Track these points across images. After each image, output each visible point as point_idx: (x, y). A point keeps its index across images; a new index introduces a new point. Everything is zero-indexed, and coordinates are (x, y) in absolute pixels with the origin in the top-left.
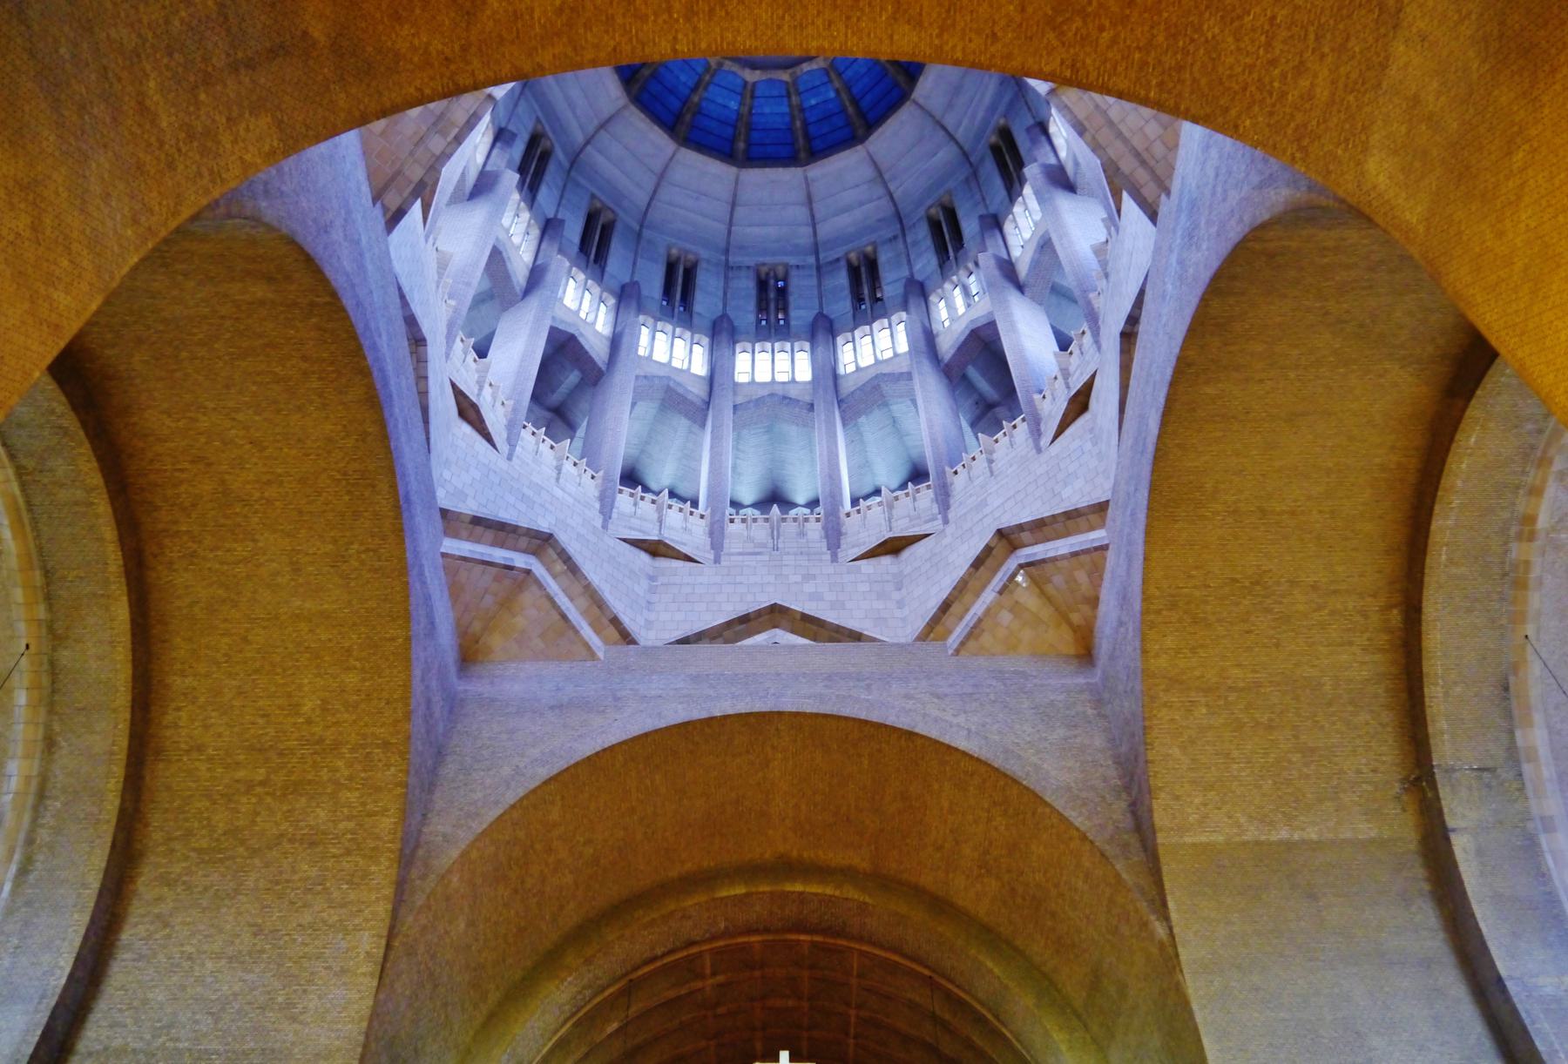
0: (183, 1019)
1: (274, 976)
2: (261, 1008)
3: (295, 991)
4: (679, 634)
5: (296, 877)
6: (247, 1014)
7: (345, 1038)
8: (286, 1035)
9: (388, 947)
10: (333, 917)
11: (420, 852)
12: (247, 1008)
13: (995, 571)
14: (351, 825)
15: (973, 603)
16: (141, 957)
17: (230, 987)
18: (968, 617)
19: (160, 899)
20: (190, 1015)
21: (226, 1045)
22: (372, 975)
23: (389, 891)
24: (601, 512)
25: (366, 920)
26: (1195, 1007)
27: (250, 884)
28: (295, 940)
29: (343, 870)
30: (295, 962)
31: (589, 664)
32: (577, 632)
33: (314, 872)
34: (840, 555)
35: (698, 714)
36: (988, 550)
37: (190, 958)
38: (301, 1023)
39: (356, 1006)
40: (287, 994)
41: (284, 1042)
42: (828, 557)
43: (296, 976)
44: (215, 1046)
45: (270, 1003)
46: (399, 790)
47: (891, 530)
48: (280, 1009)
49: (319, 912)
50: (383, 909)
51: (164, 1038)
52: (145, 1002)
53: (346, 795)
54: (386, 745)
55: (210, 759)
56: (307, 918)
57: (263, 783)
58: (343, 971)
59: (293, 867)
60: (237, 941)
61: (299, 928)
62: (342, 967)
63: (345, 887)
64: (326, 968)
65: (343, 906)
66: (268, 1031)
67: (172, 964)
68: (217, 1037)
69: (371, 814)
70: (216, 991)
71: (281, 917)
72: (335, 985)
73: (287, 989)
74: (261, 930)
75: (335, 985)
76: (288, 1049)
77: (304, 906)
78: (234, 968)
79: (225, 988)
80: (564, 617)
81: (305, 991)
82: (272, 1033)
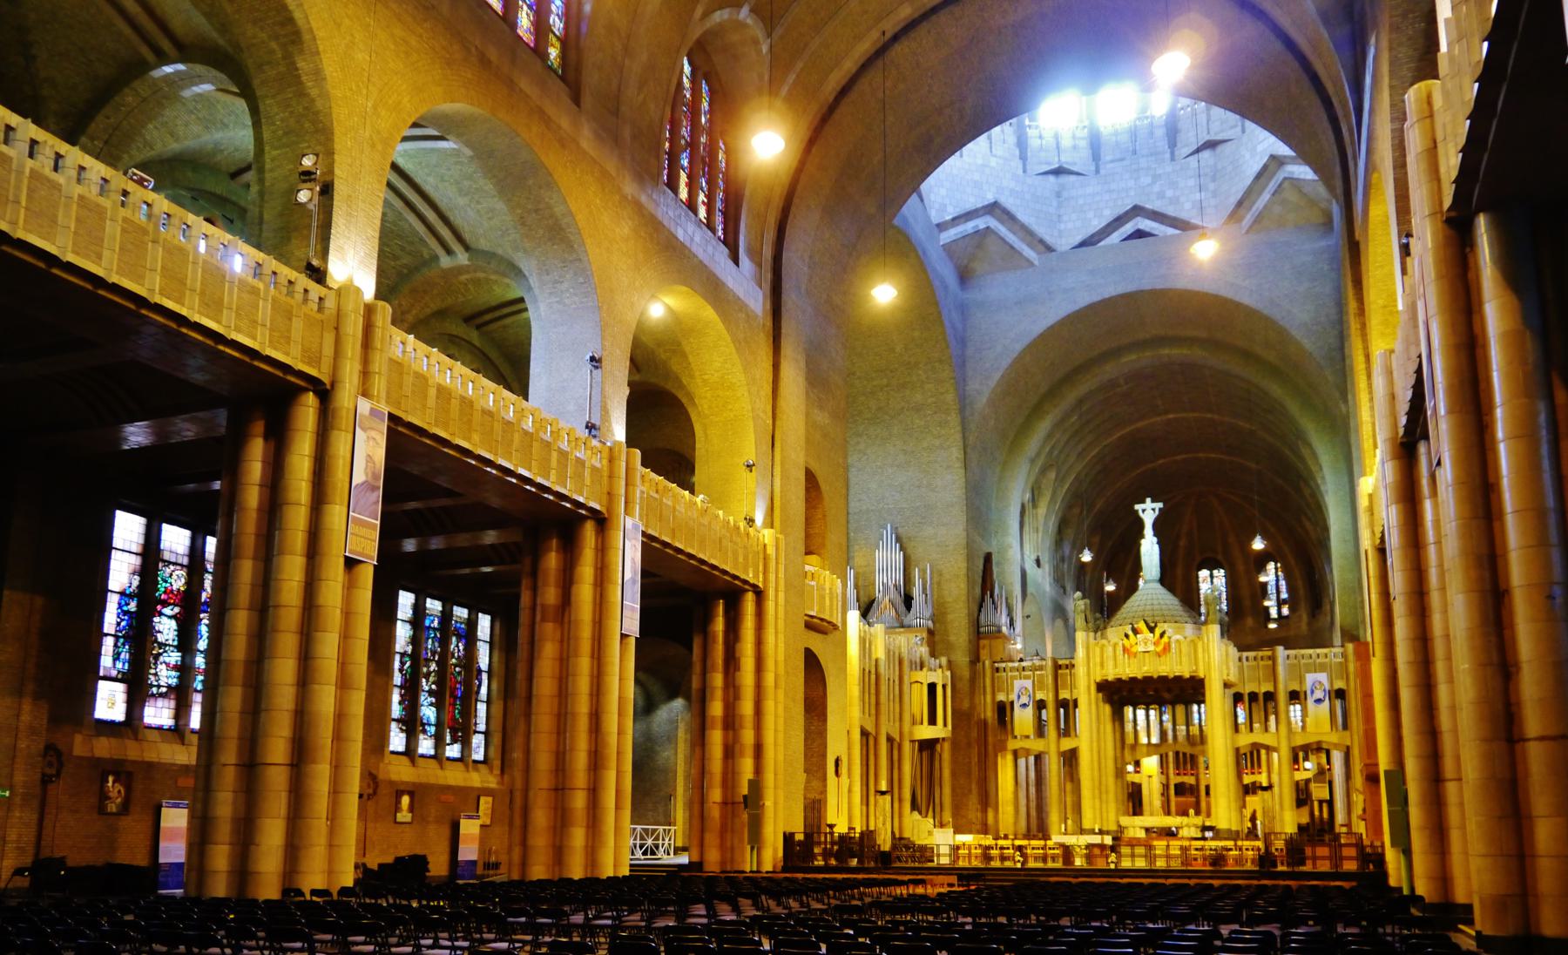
4: (1078, 239)
9: (965, 453)
10: (937, 442)
11: (967, 401)
13: (1270, 179)
14: (933, 399)
15: (1257, 200)
16: (859, 470)
18: (1254, 209)
19: (858, 443)
23: (959, 428)
24: (1021, 158)
27: (895, 431)
31: (1030, 270)
32: (1020, 254)
33: (923, 423)
34: (1177, 153)
35: (1096, 298)
36: (1265, 167)
37: (880, 468)
42: (1168, 156)
44: (904, 506)
46: (952, 381)
47: (1209, 133)
50: (958, 436)
52: (869, 489)
53: (928, 386)
54: (941, 361)
55: (859, 378)
56: (925, 444)
57: (887, 386)
58: (948, 467)
69: (942, 394)
80: (1012, 247)
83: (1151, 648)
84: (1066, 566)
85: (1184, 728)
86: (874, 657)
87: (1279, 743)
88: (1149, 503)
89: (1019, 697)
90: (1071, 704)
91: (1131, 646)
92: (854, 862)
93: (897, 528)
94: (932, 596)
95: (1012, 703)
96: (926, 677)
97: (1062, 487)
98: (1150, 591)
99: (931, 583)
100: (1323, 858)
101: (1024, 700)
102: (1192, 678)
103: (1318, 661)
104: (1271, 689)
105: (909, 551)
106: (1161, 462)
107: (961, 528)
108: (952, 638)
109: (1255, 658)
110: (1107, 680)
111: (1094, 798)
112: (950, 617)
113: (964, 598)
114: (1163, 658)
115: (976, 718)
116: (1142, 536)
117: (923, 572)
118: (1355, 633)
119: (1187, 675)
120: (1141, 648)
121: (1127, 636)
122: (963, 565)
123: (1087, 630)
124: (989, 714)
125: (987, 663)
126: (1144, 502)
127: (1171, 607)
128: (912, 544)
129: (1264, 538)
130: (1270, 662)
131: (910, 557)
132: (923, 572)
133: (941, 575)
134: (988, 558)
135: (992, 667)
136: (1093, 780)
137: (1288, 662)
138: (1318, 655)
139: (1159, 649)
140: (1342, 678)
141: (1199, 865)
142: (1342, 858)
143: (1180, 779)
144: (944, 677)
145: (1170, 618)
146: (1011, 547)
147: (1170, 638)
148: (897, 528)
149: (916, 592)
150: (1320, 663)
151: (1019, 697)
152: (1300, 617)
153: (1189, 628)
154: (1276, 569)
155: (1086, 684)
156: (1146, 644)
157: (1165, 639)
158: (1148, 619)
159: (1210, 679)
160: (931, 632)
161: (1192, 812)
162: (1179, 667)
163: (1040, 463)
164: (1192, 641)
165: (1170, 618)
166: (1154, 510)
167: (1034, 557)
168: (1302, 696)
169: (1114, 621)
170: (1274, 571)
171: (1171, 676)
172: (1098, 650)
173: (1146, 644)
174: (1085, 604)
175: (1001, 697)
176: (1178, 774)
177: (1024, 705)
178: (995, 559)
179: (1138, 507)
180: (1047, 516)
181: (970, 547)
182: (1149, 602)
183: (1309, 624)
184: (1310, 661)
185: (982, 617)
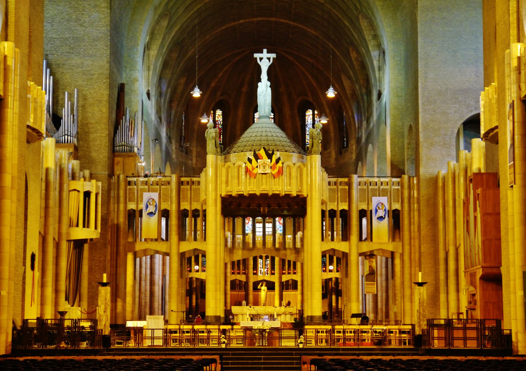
1: (69, 8)
3: (79, 14)
6: (63, 23)
8: (80, 32)
12: (62, 20)
17: (53, 12)
22: (107, 7)
26: (419, 25)
30: (75, 2)
38: (84, 27)
39: (103, 20)
41: (80, 34)
43: (78, 8)
44: (54, 36)
45: (70, 18)
58: (96, 6)
62: (95, 4)
64: (88, 5)
66: (73, 30)
68: (55, 32)
70: (48, 13)
72: (93, 11)
76: (82, 37)
78: (52, 4)
79: (51, 12)
81: (82, 14)
83: (268, 171)
84: (162, 101)
85: (241, 237)
86: (45, 166)
87: (350, 250)
88: (265, 54)
89: (147, 207)
90: (137, 214)
91: (253, 169)
92: (84, 345)
93: (47, 55)
94: (78, 117)
95: (141, 211)
96: (82, 185)
97: (170, 34)
98: (264, 125)
99: (78, 106)
100: (471, 339)
101: (151, 209)
102: (298, 196)
103: (382, 187)
104: (346, 208)
106: (242, 21)
107: (105, 60)
108: (94, 154)
109: (336, 183)
110: (231, 196)
111: (216, 291)
112: (92, 136)
113: (105, 121)
114: (277, 180)
115: (110, 223)
116: (260, 80)
117: (71, 96)
118: (401, 167)
119: (294, 194)
120: (260, 171)
121: (250, 160)
122: (106, 92)
123: (216, 154)
124: (122, 220)
125: (122, 177)
126: (262, 52)
127: (281, 139)
128: (61, 70)
129: (335, 89)
130: (347, 187)
131: (58, 80)
132: (71, 96)
133: (85, 99)
134: (122, 88)
135: (125, 180)
136: (216, 276)
137: (359, 187)
138: (382, 183)
139: (276, 171)
140: (398, 202)
141: (367, 344)
142: (453, 339)
143: (234, 277)
144: (97, 187)
145: (281, 148)
146: (137, 81)
147: (283, 164)
148: (47, 55)
149: (65, 112)
150: (382, 189)
151: (147, 207)
152: (330, 153)
153: (295, 157)
154: (313, 115)
155: (214, 197)
156: (264, 167)
157: (280, 164)
158: (266, 147)
159: (311, 198)
160: (76, 148)
161: (244, 302)
162: (289, 187)
163: (159, 11)
164: (299, 167)
165: (281, 148)
166: (269, 59)
167: (145, 92)
168: (369, 213)
169: (236, 147)
170: (311, 117)
171: (270, 194)
172: (224, 171)
173: (264, 167)
174: (216, 132)
175: (132, 206)
176: (233, 273)
177: (151, 214)
178: (127, 89)
179: (257, 56)
180: (157, 57)
181: (111, 76)
182: (264, 134)
183: (336, 159)
184: (376, 187)
185: (118, 138)
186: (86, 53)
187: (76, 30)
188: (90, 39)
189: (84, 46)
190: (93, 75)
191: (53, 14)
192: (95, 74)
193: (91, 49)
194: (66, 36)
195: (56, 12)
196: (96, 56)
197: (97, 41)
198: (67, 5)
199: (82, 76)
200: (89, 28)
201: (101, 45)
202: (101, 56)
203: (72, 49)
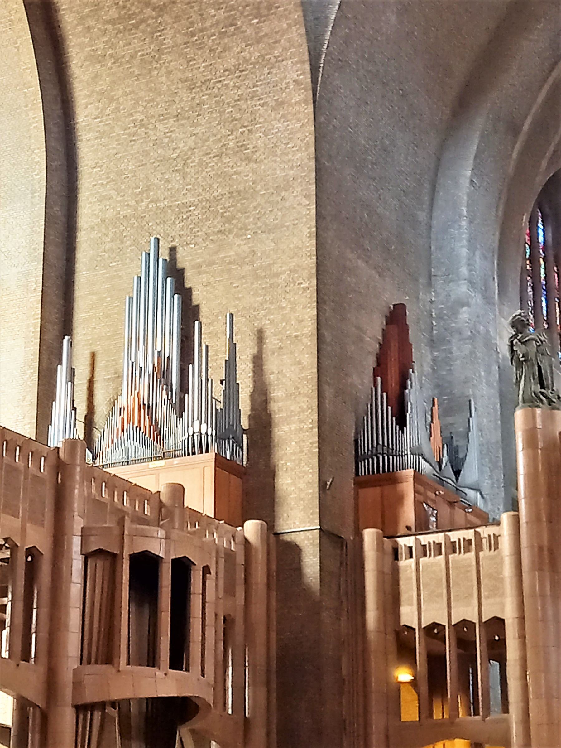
0: (156, 181)
2: (217, 156)
3: (242, 133)
5: (208, 24)
7: (297, 167)
8: (247, 176)
10: (253, 53)
20: (159, 176)
21: (198, 196)
25: (285, 49)
28: (227, 85)
29: (247, 6)
30: (232, 107)
40: (236, 138)
41: (246, 181)
44: (190, 199)
48: (234, 153)
49: (238, 53)
51: (146, 201)
58: (280, 104)
59: (201, 15)
60: (177, 99)
61: (227, 73)
63: (256, 21)
65: (258, 42)
67: (130, 135)
70: (174, 149)
71: (207, 66)
72: (275, 119)
73: (235, 133)
74: (195, 84)
75: (275, 119)
76: (250, 187)
77: (224, 50)
78: (183, 125)
81: (250, 131)
82: (234, 177)
105: (197, 297)
107: (306, 231)
186: (259, 224)
187: (236, 173)
188: (268, 189)
189: (255, 208)
190: (277, 275)
191: (186, 148)
192: (281, 273)
193: (271, 211)
194: (216, 194)
195: (191, 142)
196: (283, 226)
197: (285, 190)
198: (215, 119)
199: (252, 284)
200: (266, 161)
201: (295, 197)
202: (294, 225)
203: (229, 220)
